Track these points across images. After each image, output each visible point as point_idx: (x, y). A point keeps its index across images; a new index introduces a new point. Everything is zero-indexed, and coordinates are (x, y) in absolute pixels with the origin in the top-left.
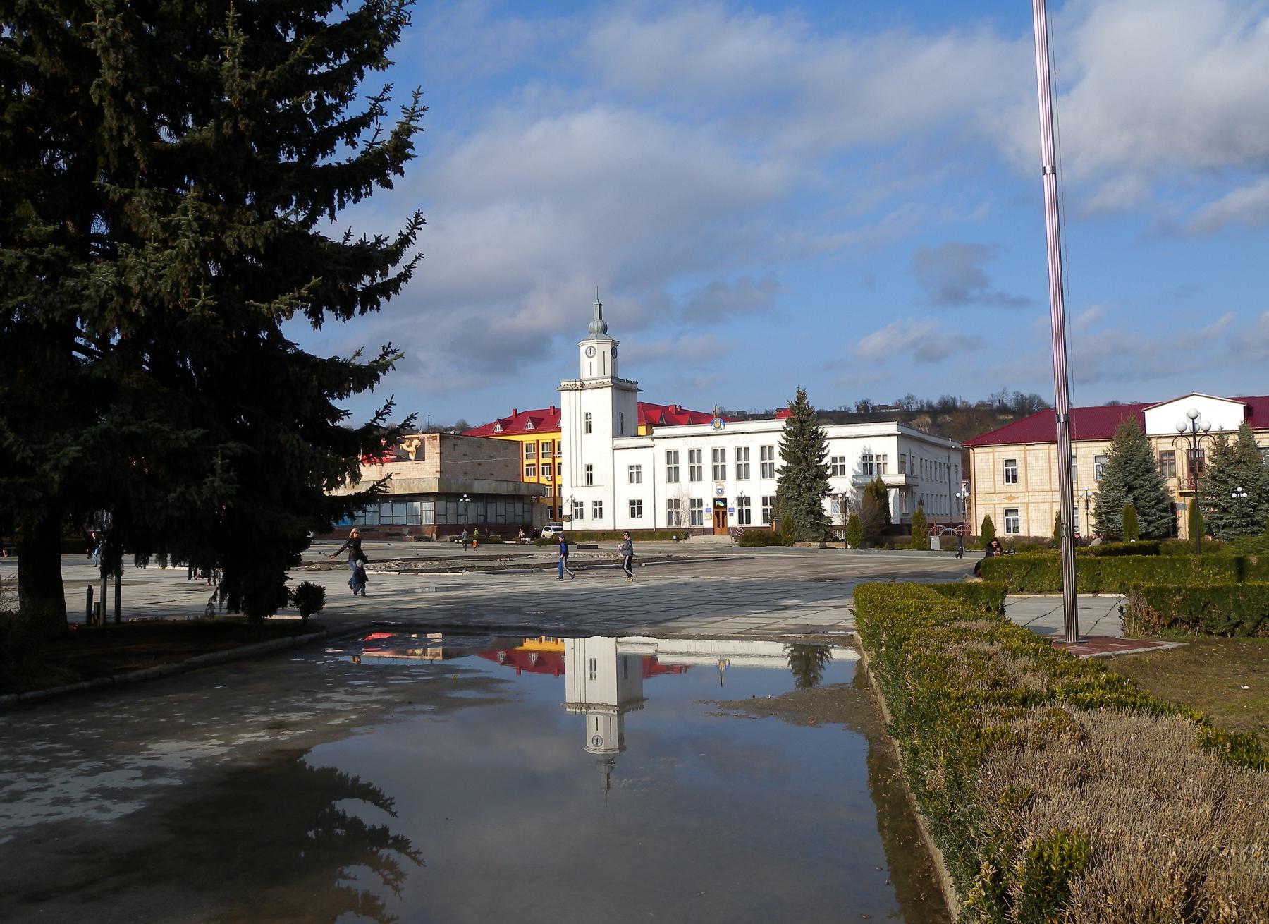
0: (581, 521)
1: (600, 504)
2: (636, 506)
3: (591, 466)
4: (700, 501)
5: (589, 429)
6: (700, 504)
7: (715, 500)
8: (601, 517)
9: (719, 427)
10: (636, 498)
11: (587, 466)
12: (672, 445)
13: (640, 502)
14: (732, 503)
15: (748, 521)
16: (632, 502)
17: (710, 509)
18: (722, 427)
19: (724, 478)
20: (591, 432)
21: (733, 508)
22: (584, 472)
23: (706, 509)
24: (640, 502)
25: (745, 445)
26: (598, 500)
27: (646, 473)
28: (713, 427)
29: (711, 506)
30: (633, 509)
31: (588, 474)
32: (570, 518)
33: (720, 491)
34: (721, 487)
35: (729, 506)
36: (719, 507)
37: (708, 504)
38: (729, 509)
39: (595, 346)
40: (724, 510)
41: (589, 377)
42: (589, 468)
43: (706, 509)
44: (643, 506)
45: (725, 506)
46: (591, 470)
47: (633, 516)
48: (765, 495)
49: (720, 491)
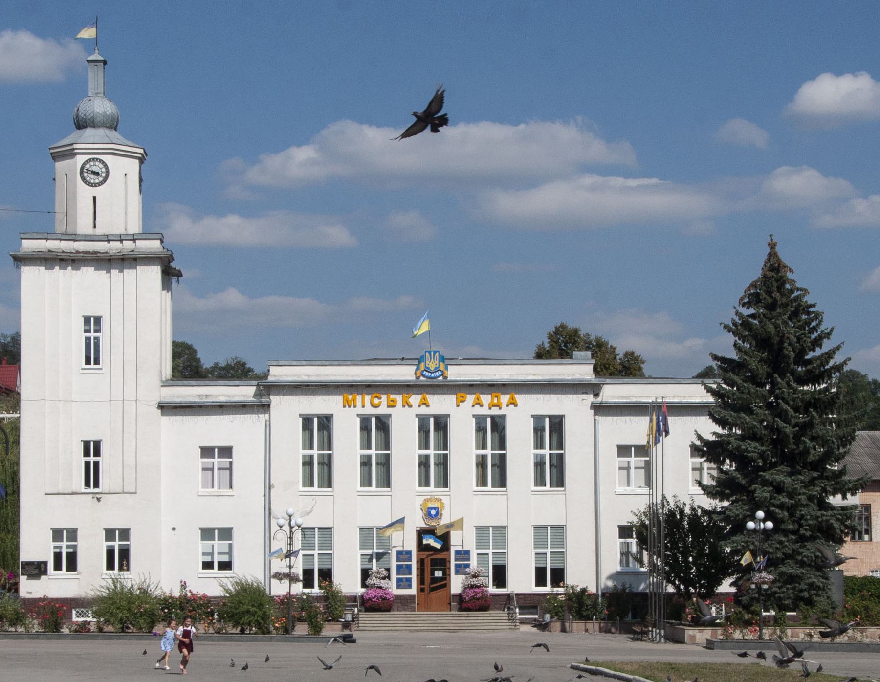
1: (125, 534)
3: (97, 444)
5: (92, 356)
7: (421, 534)
11: (86, 444)
12: (318, 404)
17: (409, 553)
19: (444, 482)
20: (97, 362)
21: (467, 553)
22: (81, 460)
23: (399, 553)
25: (495, 411)
29: (411, 545)
31: (87, 464)
32: (37, 570)
33: (433, 512)
34: (435, 505)
36: (429, 548)
38: (457, 553)
39: (107, 159)
42: (92, 448)
43: (399, 553)
45: (446, 547)
46: (97, 453)
49: (433, 512)
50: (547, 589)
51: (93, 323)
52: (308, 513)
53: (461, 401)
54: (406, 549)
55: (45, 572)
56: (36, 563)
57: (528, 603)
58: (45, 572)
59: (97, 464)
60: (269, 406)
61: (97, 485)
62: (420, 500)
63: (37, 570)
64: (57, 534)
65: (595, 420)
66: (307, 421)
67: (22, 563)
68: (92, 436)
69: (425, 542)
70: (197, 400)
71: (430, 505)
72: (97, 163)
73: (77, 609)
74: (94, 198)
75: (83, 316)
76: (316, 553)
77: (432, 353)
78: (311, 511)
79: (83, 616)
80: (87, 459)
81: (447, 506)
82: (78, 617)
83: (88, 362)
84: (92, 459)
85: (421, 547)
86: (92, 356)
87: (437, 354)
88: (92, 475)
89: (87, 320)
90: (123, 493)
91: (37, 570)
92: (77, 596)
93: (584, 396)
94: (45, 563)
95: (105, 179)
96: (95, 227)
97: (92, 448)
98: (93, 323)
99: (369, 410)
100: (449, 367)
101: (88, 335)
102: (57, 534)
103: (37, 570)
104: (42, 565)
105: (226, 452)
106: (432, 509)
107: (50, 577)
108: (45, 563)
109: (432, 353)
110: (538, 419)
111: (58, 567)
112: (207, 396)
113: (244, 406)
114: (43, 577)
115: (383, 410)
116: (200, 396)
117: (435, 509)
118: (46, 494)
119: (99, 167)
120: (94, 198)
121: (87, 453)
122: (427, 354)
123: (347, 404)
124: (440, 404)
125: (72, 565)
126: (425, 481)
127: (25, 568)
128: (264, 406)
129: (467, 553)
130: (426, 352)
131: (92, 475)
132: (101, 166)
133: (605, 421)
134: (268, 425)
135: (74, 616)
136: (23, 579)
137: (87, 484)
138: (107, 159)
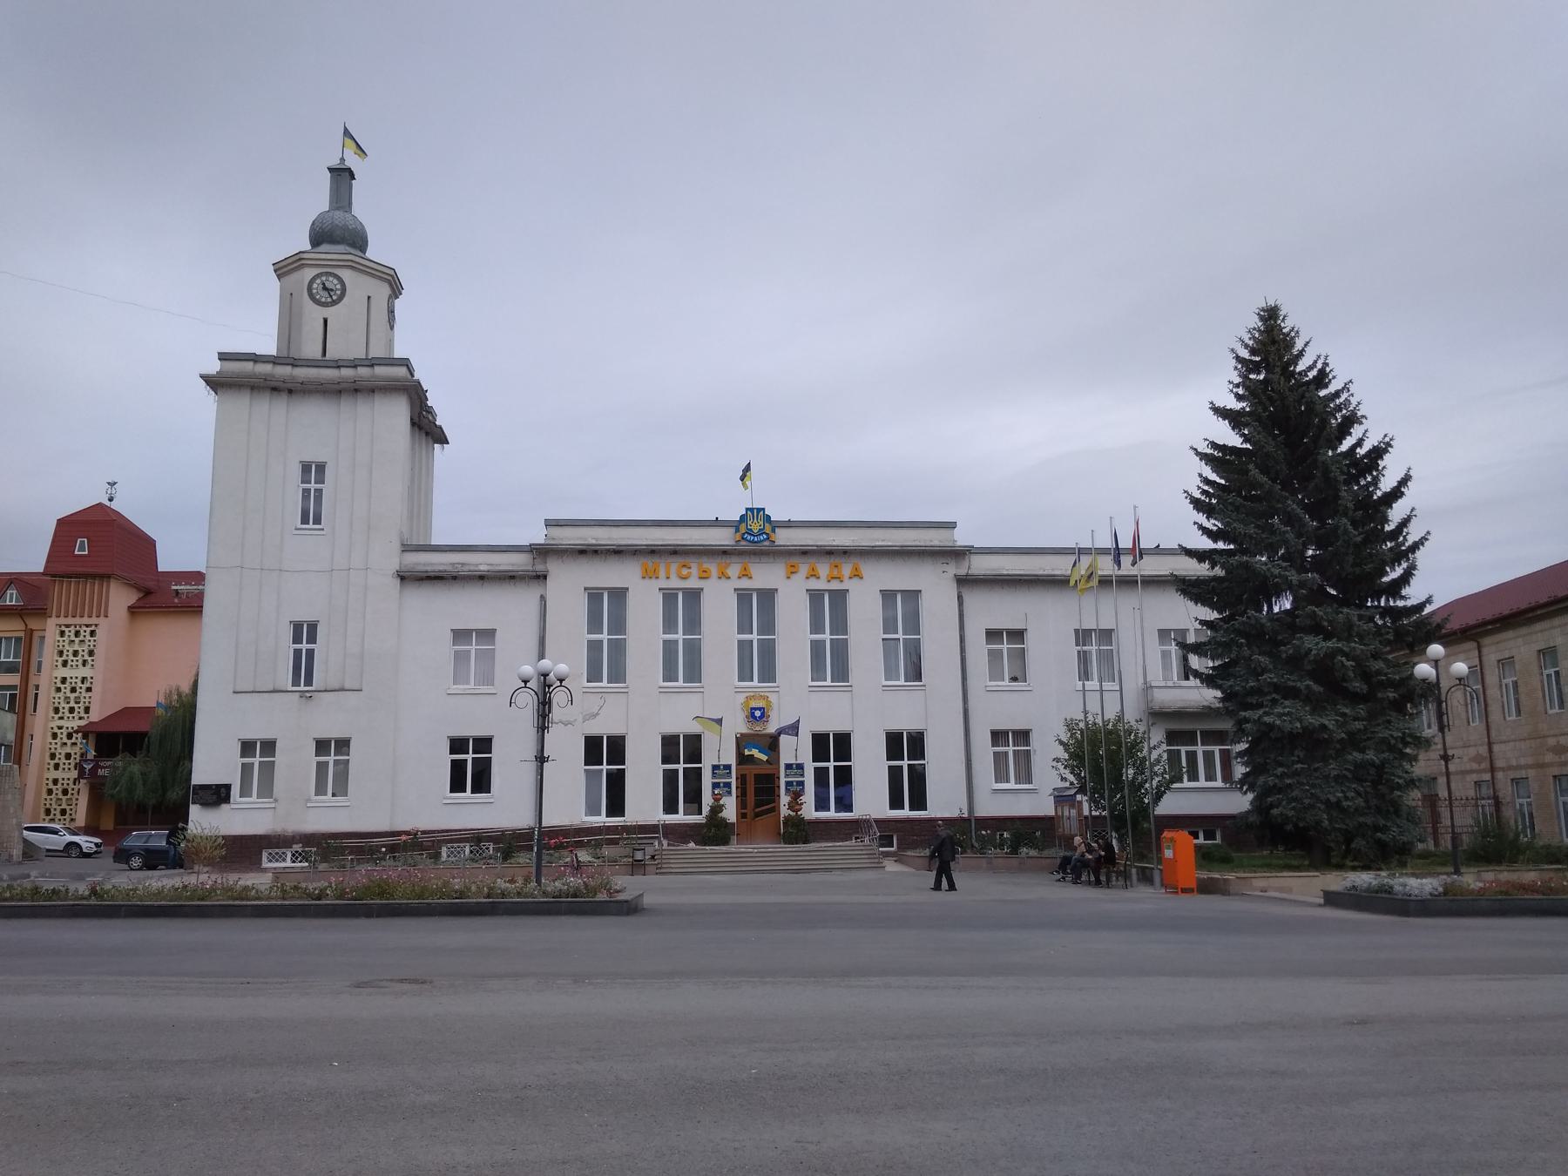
0: (266, 802)
2: (469, 757)
3: (313, 627)
4: (694, 746)
6: (695, 754)
7: (742, 742)
8: (341, 788)
10: (471, 729)
11: (297, 627)
12: (608, 575)
13: (484, 744)
14: (798, 750)
15: (845, 803)
16: (458, 745)
17: (728, 767)
19: (768, 674)
20: (317, 520)
21: (800, 767)
23: (715, 767)
24: (484, 744)
25: (835, 585)
26: (332, 732)
29: (730, 758)
30: (458, 769)
31: (297, 653)
32: (217, 795)
33: (758, 713)
34: (761, 704)
35: (786, 757)
37: (719, 751)
38: (788, 766)
39: (346, 275)
40: (767, 770)
43: (715, 767)
44: (497, 756)
46: (312, 639)
47: (457, 785)
48: (895, 726)
49: (758, 713)
50: (906, 813)
51: (313, 471)
52: (595, 715)
53: (792, 571)
54: (723, 762)
55: (227, 799)
56: (214, 787)
57: (887, 831)
58: (227, 799)
59: (310, 653)
60: (545, 577)
61: (309, 682)
62: (741, 698)
63: (215, 797)
64: (247, 747)
65: (960, 598)
66: (594, 596)
67: (195, 786)
68: (305, 616)
69: (747, 752)
70: (449, 568)
71: (754, 704)
72: (331, 279)
73: (270, 851)
74: (325, 321)
75: (301, 462)
77: (755, 511)
78: (597, 714)
79: (277, 861)
80: (298, 646)
81: (775, 706)
82: (270, 861)
83: (305, 520)
84: (304, 646)
85: (743, 759)
86: (311, 515)
87: (762, 512)
88: (303, 668)
89: (306, 468)
90: (343, 690)
91: (217, 795)
92: (269, 833)
93: (945, 567)
94: (228, 787)
97: (305, 631)
98: (313, 471)
99: (675, 583)
100: (777, 530)
102: (247, 747)
103: (215, 797)
104: (223, 790)
106: (755, 709)
107: (233, 806)
108: (228, 787)
109: (755, 511)
110: (888, 596)
111: (245, 791)
112: (463, 564)
113: (512, 577)
114: (224, 807)
116: (453, 564)
117: (760, 709)
118: (234, 692)
119: (332, 283)
120: (325, 321)
121: (297, 639)
122: (749, 512)
123: (648, 575)
124: (765, 575)
125: (267, 789)
126: (745, 674)
127: (197, 794)
128: (538, 577)
129: (800, 767)
130: (747, 509)
131: (303, 668)
132: (335, 281)
133: (975, 600)
134: (543, 598)
136: (194, 810)
137: (296, 682)
138: (346, 275)
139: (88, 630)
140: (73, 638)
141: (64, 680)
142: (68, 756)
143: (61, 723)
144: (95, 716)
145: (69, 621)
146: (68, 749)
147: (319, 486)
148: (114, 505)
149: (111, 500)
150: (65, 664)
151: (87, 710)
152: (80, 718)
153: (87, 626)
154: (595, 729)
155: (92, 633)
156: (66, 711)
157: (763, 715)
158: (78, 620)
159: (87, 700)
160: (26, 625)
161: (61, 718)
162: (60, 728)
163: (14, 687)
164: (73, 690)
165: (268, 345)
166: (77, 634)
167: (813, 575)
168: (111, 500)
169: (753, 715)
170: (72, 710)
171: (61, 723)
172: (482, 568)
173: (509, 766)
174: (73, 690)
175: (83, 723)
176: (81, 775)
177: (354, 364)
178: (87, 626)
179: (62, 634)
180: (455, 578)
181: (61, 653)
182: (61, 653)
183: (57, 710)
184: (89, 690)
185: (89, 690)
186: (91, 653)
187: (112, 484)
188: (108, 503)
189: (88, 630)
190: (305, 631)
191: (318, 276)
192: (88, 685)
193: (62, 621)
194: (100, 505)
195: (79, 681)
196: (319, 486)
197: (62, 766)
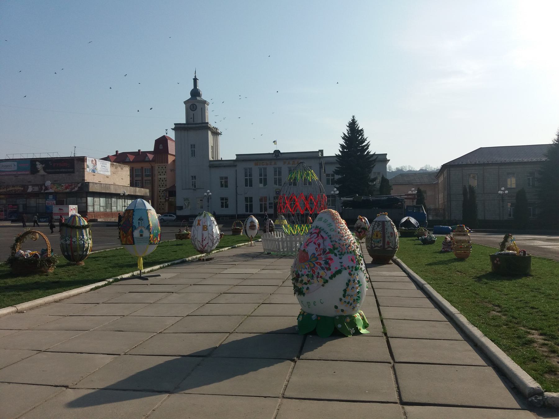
9: (278, 155)
16: (222, 199)
17: (272, 203)
18: (280, 155)
23: (269, 203)
24: (226, 199)
27: (231, 182)
28: (274, 155)
30: (222, 203)
31: (193, 182)
33: (278, 192)
34: (278, 191)
39: (197, 104)
41: (193, 123)
43: (269, 203)
76: (249, 203)
86: (193, 154)
89: (192, 145)
91: (181, 208)
95: (196, 109)
96: (194, 121)
99: (261, 166)
101: (192, 149)
105: (226, 178)
114: (182, 210)
115: (264, 166)
118: (182, 189)
123: (256, 164)
124: (280, 164)
134: (236, 170)
135: (189, 220)
139: (164, 166)
140: (161, 169)
141: (160, 179)
142: (163, 196)
143: (160, 188)
144: (168, 187)
145: (160, 164)
146: (163, 195)
147: (194, 149)
148: (167, 135)
149: (167, 134)
150: (160, 175)
151: (166, 185)
152: (165, 187)
153: (164, 166)
154: (247, 196)
155: (165, 167)
156: (161, 186)
157: (279, 193)
158: (162, 164)
159: (166, 183)
160: (151, 165)
161: (160, 187)
162: (160, 190)
163: (150, 180)
164: (163, 181)
165: (183, 121)
166: (162, 168)
167: (289, 163)
168: (167, 134)
169: (277, 193)
170: (163, 186)
171: (160, 188)
172: (225, 164)
173: (231, 203)
174: (163, 181)
175: (165, 188)
176: (166, 201)
177: (199, 124)
178: (164, 166)
179: (159, 168)
180: (220, 167)
181: (159, 172)
182: (159, 172)
183: (159, 186)
184: (166, 181)
185: (166, 181)
186: (166, 172)
187: (167, 130)
188: (166, 135)
189: (164, 166)
190: (194, 177)
191: (192, 105)
192: (165, 180)
193: (159, 164)
194: (164, 136)
195: (164, 179)
196: (194, 149)
197: (162, 198)
